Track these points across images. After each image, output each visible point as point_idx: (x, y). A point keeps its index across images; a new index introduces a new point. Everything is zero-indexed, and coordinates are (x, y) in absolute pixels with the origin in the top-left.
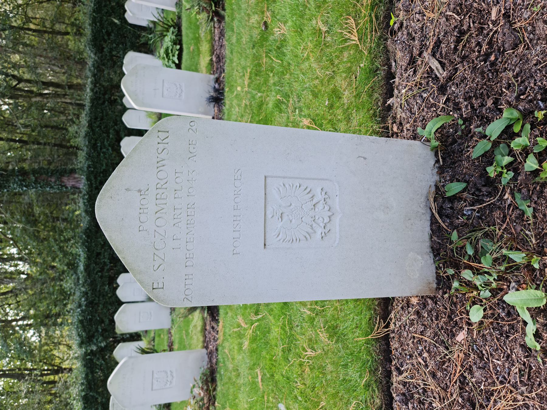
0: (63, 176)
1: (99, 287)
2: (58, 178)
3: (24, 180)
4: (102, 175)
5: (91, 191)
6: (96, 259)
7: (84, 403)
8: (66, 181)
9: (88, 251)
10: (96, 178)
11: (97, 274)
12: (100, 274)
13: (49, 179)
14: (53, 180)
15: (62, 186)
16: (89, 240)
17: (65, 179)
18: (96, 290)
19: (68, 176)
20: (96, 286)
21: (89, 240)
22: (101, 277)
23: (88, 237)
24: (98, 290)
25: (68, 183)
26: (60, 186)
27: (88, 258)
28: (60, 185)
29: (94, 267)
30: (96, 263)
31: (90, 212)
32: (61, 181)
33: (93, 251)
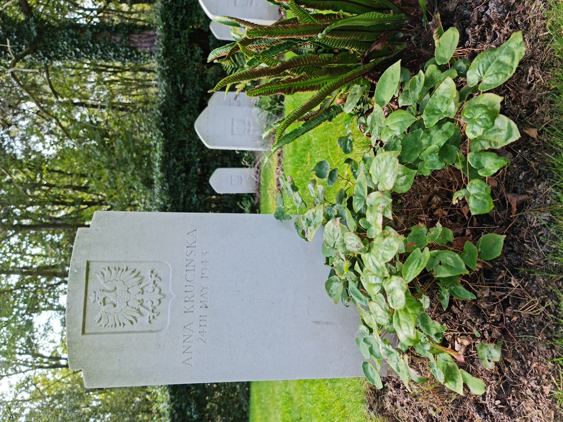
0: (133, 33)
1: (182, 196)
2: (126, 35)
3: (77, 37)
4: (184, 11)
5: (168, 38)
6: (178, 152)
7: (171, 394)
8: (136, 40)
9: (165, 136)
10: (176, 19)
11: (179, 174)
12: (184, 175)
13: (113, 37)
14: (118, 39)
15: (132, 49)
16: (166, 119)
17: (135, 38)
18: (178, 201)
19: (139, 33)
20: (179, 194)
21: (166, 119)
22: (186, 181)
23: (165, 114)
24: (181, 201)
25: (139, 44)
26: (128, 49)
27: (166, 148)
28: (128, 47)
29: (174, 164)
30: (178, 159)
31: (167, 70)
32: (129, 40)
33: (173, 139)
